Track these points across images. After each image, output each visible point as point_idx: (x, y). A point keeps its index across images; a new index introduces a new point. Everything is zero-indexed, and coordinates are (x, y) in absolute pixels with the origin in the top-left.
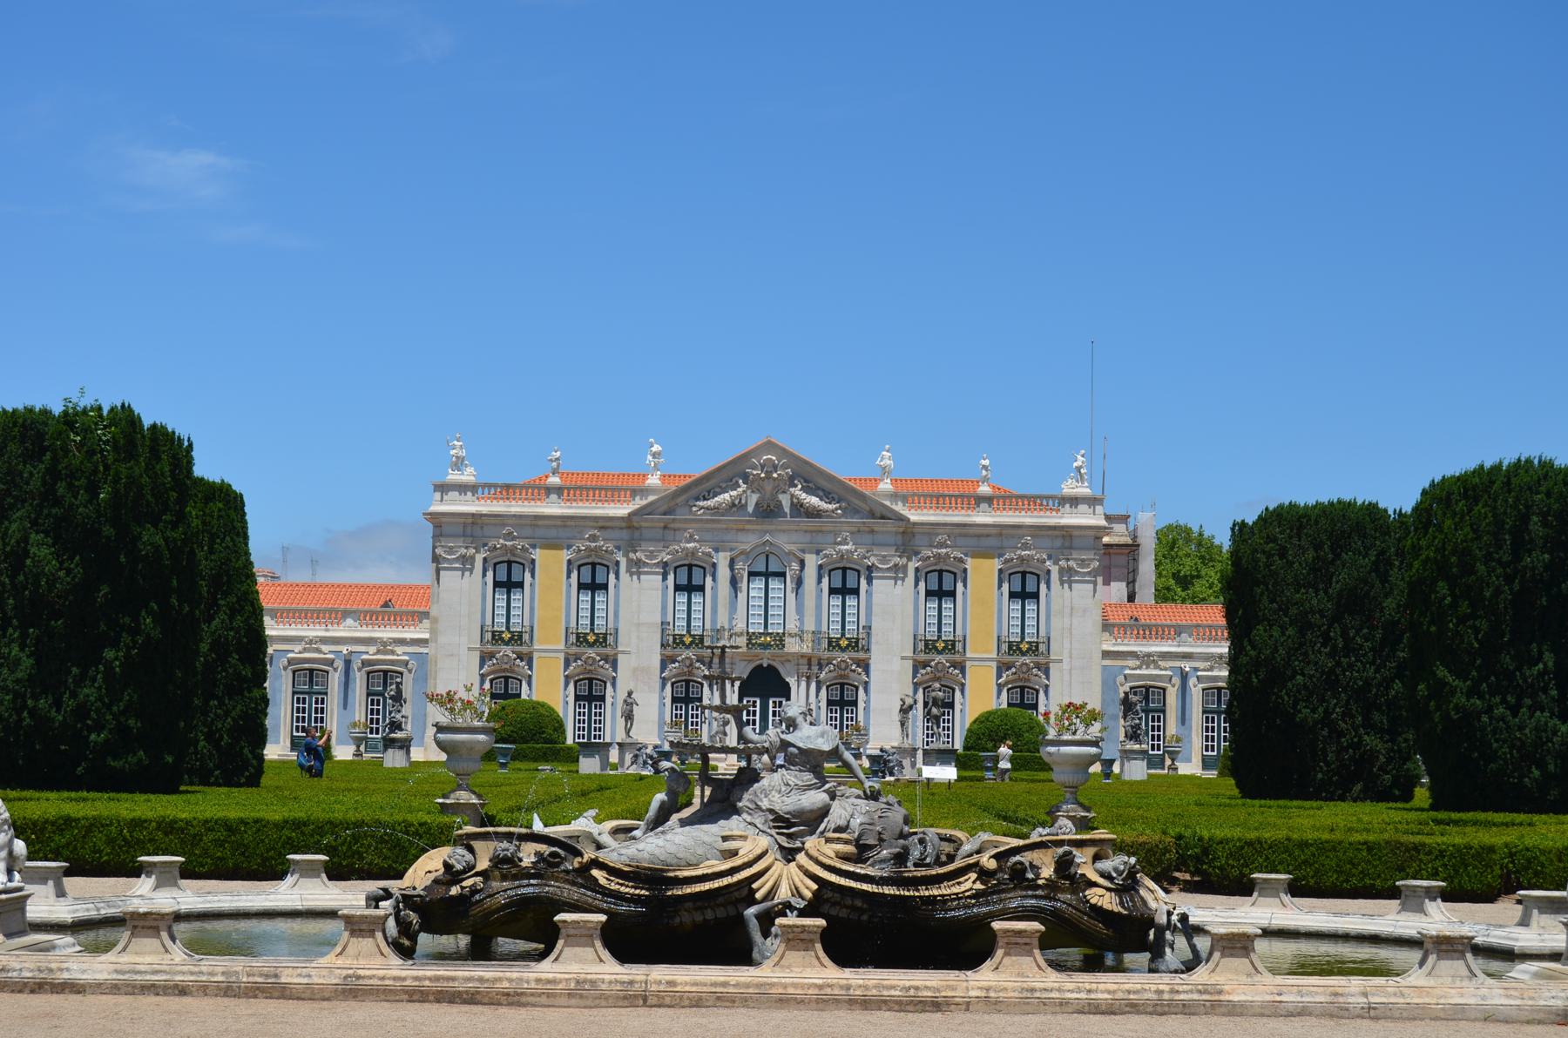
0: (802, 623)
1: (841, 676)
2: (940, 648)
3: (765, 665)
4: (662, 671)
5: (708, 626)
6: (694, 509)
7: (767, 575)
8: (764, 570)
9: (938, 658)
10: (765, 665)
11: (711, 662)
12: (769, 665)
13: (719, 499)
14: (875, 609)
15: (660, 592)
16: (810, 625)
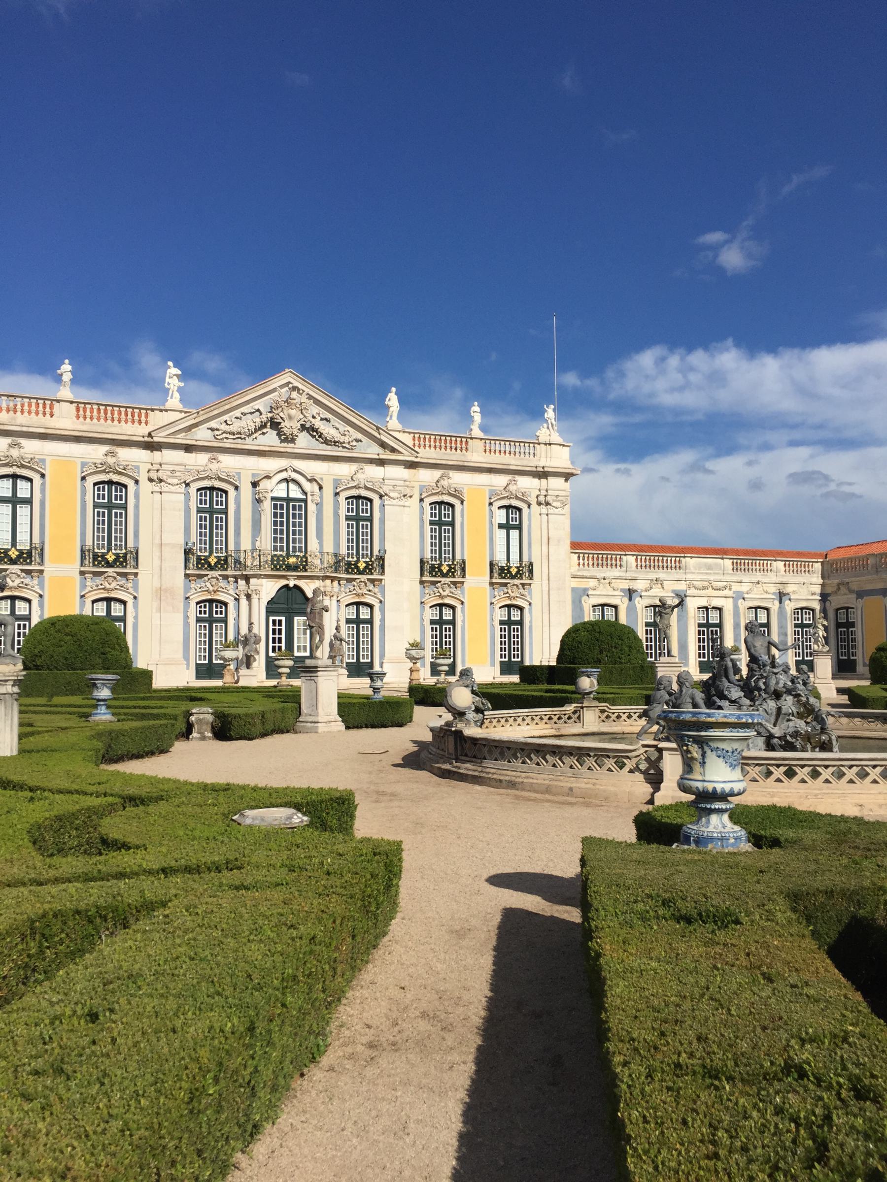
0: (321, 544)
1: (358, 595)
2: (445, 571)
3: (291, 585)
4: (187, 589)
5: (231, 547)
6: (217, 433)
7: (288, 500)
8: (285, 496)
9: (443, 580)
10: (291, 585)
11: (236, 582)
12: (295, 586)
13: (243, 423)
14: (387, 535)
15: (183, 513)
16: (329, 548)
